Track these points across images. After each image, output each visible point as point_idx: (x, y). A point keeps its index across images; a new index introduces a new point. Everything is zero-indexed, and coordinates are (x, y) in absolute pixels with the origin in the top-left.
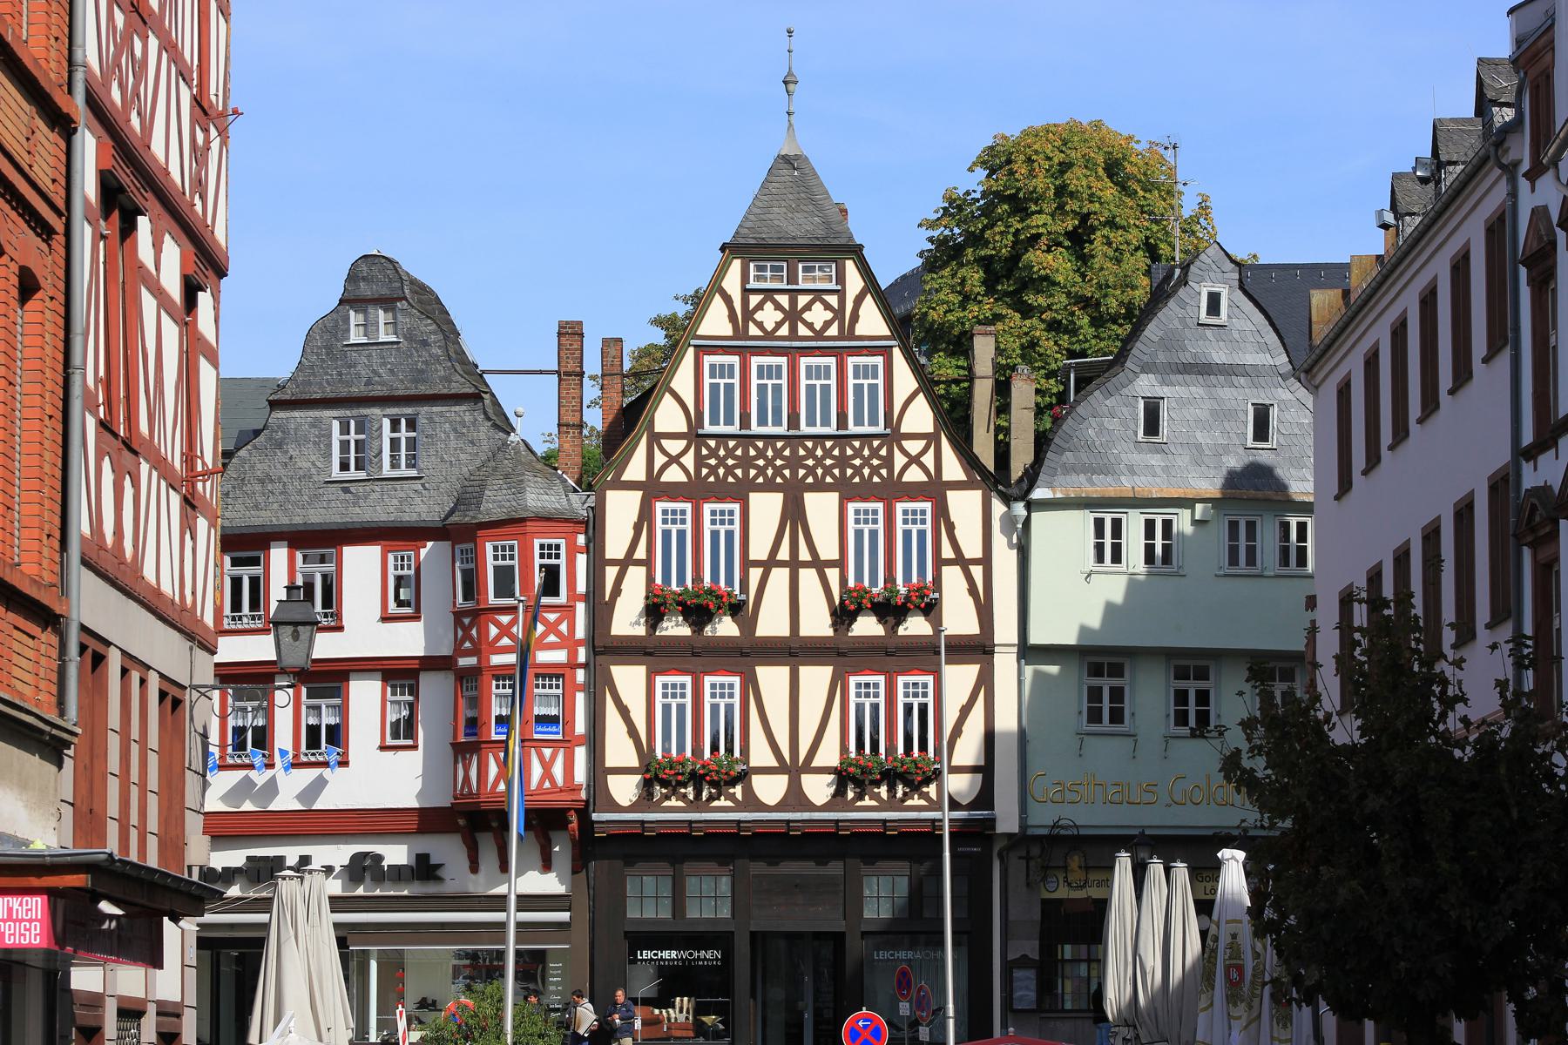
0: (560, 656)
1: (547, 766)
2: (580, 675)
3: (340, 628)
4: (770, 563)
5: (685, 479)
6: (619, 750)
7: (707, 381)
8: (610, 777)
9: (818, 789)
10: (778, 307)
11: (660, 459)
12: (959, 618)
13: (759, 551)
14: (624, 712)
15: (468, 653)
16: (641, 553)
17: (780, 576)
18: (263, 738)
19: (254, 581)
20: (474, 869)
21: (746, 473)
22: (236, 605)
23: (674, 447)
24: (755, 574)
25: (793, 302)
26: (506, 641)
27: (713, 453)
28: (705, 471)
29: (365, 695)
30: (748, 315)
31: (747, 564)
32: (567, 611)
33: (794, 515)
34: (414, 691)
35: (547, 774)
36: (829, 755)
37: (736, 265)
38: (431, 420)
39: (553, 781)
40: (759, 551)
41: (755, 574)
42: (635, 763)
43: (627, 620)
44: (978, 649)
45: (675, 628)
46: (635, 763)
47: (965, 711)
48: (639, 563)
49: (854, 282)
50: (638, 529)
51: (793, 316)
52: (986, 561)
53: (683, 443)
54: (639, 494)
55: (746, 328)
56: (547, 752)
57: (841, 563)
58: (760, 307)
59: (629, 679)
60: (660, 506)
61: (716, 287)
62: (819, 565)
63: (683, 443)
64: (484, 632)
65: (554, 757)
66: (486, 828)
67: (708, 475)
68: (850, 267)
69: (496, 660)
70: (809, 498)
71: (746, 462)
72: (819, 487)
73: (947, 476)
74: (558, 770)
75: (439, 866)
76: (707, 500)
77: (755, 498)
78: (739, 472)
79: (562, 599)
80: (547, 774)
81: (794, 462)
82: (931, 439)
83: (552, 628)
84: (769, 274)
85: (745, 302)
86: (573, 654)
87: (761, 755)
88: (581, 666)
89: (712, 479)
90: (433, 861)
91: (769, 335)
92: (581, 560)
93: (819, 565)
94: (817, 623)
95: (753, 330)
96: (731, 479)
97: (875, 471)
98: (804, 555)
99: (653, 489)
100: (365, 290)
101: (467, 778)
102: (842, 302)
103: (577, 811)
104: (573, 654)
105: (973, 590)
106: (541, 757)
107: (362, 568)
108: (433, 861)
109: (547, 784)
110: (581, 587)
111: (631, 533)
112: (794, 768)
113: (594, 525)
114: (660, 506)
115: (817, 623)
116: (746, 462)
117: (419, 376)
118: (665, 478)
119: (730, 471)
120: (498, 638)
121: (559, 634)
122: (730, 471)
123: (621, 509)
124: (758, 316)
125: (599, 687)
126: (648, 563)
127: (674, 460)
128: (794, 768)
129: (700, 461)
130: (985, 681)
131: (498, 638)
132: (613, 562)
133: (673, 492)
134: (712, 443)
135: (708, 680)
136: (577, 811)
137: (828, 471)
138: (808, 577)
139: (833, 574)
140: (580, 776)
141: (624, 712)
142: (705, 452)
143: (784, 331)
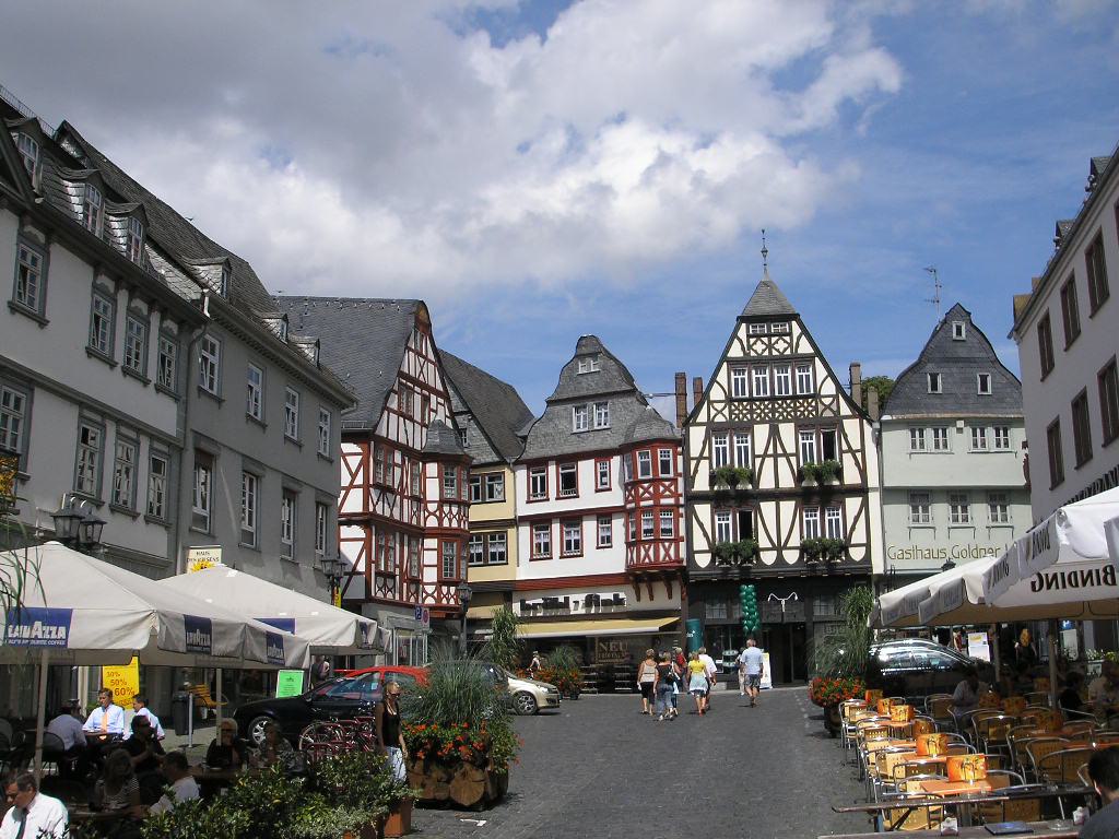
0: (671, 501)
1: (667, 551)
2: (682, 510)
4: (765, 455)
6: (700, 543)
9: (791, 557)
10: (763, 342)
11: (713, 412)
12: (851, 476)
13: (759, 450)
14: (701, 525)
15: (630, 502)
16: (706, 454)
17: (769, 462)
19: (543, 479)
20: (639, 600)
22: (535, 490)
23: (719, 406)
24: (758, 461)
25: (770, 341)
26: (647, 495)
29: (590, 527)
30: (750, 347)
31: (754, 456)
32: (674, 481)
33: (774, 434)
34: (610, 522)
35: (667, 554)
36: (795, 541)
39: (670, 558)
40: (759, 450)
41: (758, 461)
43: (702, 484)
44: (861, 491)
47: (856, 519)
48: (705, 458)
49: (796, 330)
50: (704, 443)
51: (770, 346)
52: (863, 450)
56: (667, 544)
57: (797, 455)
58: (755, 343)
62: (786, 455)
64: (637, 492)
65: (670, 547)
66: (642, 581)
68: (794, 323)
69: (643, 504)
70: (782, 427)
72: (785, 420)
73: (842, 413)
74: (672, 552)
79: (671, 475)
80: (667, 554)
81: (773, 411)
82: (835, 397)
85: (748, 342)
86: (677, 500)
87: (763, 542)
88: (682, 506)
92: (680, 458)
93: (786, 455)
94: (787, 482)
95: (753, 354)
97: (810, 412)
98: (780, 451)
100: (584, 350)
102: (792, 339)
104: (677, 500)
105: (857, 463)
106: (664, 547)
107: (586, 470)
110: (680, 470)
112: (779, 548)
113: (684, 442)
115: (787, 482)
116: (751, 411)
117: (607, 385)
118: (716, 420)
119: (745, 416)
120: (643, 494)
121: (670, 491)
122: (745, 416)
123: (697, 435)
125: (691, 514)
126: (710, 458)
127: (720, 412)
128: (779, 548)
129: (731, 412)
130: (865, 505)
131: (643, 494)
132: (693, 459)
137: (789, 413)
138: (782, 461)
139: (793, 459)
140: (683, 554)
141: (701, 525)
143: (766, 353)
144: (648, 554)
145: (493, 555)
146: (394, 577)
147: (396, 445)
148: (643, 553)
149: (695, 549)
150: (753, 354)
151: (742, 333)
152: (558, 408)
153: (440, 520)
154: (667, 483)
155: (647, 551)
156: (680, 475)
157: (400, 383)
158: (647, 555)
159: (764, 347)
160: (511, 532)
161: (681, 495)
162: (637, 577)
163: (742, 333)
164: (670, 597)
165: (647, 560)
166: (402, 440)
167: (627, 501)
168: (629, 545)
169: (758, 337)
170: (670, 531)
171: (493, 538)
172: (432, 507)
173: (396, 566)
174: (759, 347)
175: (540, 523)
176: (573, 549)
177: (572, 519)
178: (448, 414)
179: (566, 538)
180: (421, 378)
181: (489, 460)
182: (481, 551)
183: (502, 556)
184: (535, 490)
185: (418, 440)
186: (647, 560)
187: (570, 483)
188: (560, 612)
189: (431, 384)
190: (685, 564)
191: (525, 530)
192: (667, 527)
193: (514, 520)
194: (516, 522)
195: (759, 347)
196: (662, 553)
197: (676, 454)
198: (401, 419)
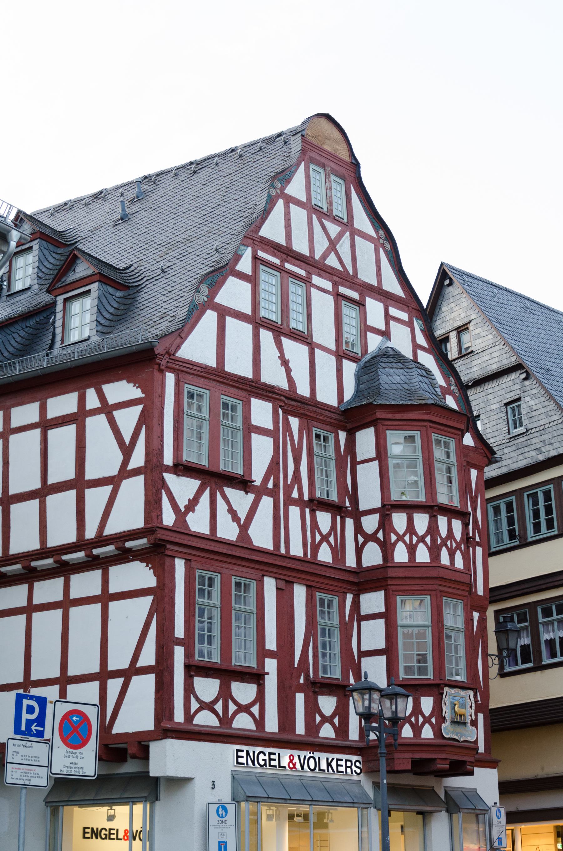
146: (256, 677)
147: (255, 388)
153: (387, 549)
157: (255, 258)
166: (273, 375)
172: (370, 523)
173: (263, 653)
178: (421, 340)
180: (332, 261)
185: (332, 385)
189: (367, 275)
198: (266, 336)
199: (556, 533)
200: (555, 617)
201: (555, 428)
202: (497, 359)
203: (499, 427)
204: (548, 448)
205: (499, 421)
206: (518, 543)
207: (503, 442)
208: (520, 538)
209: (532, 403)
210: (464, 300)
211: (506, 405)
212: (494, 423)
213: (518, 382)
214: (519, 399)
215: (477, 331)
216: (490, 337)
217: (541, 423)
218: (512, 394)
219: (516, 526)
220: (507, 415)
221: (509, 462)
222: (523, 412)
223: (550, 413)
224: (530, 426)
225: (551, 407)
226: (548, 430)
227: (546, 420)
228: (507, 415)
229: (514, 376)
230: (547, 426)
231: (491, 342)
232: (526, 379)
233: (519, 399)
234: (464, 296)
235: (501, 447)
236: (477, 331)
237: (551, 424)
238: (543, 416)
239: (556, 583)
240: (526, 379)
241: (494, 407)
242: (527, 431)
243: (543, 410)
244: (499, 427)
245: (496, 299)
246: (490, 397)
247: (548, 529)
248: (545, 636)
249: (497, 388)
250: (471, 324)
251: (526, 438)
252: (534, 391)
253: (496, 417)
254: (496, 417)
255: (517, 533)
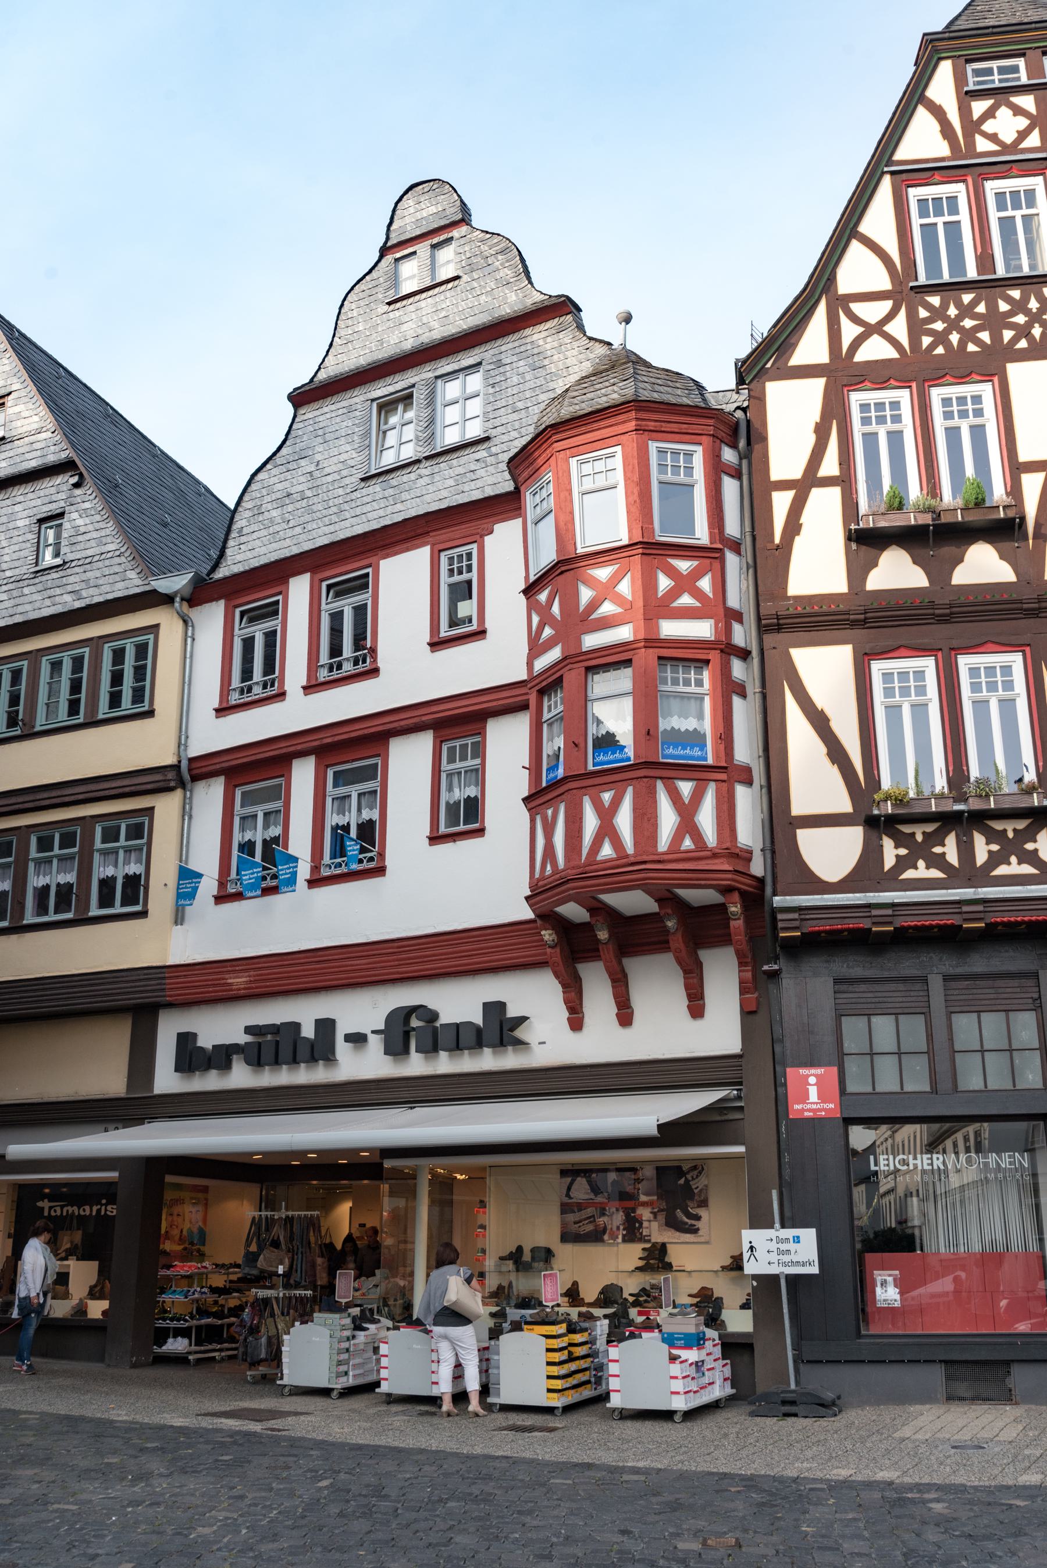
0: (702, 629)
1: (687, 812)
3: (374, 672)
5: (892, 354)
6: (814, 783)
7: (916, 222)
8: (800, 833)
10: (1018, 111)
11: (849, 331)
14: (820, 722)
16: (830, 466)
18: (273, 851)
19: (270, 637)
20: (576, 1023)
21: (996, 337)
22: (247, 673)
23: (872, 312)
27: (938, 314)
28: (926, 341)
29: (410, 761)
30: (972, 127)
34: (479, 750)
35: (687, 824)
37: (945, 70)
38: (499, 364)
42: (844, 805)
45: (896, 572)
46: (844, 805)
48: (828, 482)
50: (821, 432)
53: (887, 305)
54: (818, 384)
55: (971, 144)
56: (685, 788)
58: (990, 114)
59: (824, 668)
60: (856, 398)
61: (915, 95)
63: (887, 305)
65: (697, 797)
67: (932, 346)
69: (591, 641)
71: (994, 321)
74: (706, 819)
75: (523, 1019)
76: (938, 380)
77: (1015, 371)
78: (985, 336)
80: (687, 824)
83: (685, 583)
84: (996, 77)
85: (964, 111)
88: (744, 654)
89: (940, 350)
90: (512, 1012)
91: (1006, 148)
95: (983, 145)
96: (971, 348)
99: (842, 375)
101: (549, 848)
103: (743, 894)
106: (675, 797)
108: (512, 1012)
109: (688, 843)
111: (812, 439)
114: (856, 398)
116: (994, 321)
118: (861, 356)
121: (698, 594)
124: (988, 127)
125: (776, 681)
126: (845, 481)
127: (877, 329)
129: (916, 328)
132: (784, 485)
133: (878, 375)
134: (935, 300)
135: (965, 662)
136: (743, 894)
140: (748, 831)
141: (820, 722)
142: (923, 313)
144: (613, 825)
145: (107, 884)
148: (591, 822)
149: (799, 807)
150: (983, 145)
151: (942, 87)
152: (327, 413)
154: (684, 566)
155: (606, 816)
156: (736, 546)
158: (607, 830)
159: (1023, 123)
160: (166, 808)
161: (738, 616)
162: (582, 930)
163: (942, 87)
164: (697, 1009)
165: (607, 851)
167: (536, 648)
168: (537, 800)
169: (1001, 94)
170: (696, 738)
171: (110, 835)
174: (1006, 125)
175: (252, 770)
176: (356, 853)
177: (353, 749)
179: (332, 819)
181: (119, 590)
182: (69, 877)
183: (135, 888)
184: (247, 673)
186: (607, 851)
187: (349, 652)
188: (303, 1076)
190: (757, 868)
191: (210, 797)
192: (688, 724)
193: (176, 767)
194: (184, 775)
195: (1006, 125)
196: (668, 819)
197: (716, 470)
199: (81, 721)
200: (56, 851)
201: (107, 562)
202: (39, 453)
203: (23, 554)
204: (91, 591)
205: (24, 545)
206: (19, 732)
207: (25, 577)
208: (24, 724)
209: (80, 522)
210: (7, 362)
211: (41, 521)
212: (17, 548)
213: (65, 489)
214: (61, 515)
215: (17, 409)
216: (36, 418)
217: (89, 552)
218: (53, 506)
219: (21, 708)
220: (39, 538)
221: (28, 607)
222: (65, 535)
223: (104, 540)
224: (70, 557)
225: (108, 532)
226: (95, 565)
227: (97, 550)
228: (39, 538)
229: (59, 480)
230: (96, 558)
231: (35, 426)
232: (77, 485)
233: (61, 515)
234: (8, 356)
235: (21, 584)
236: (17, 409)
237: (103, 556)
238: (93, 543)
239: (67, 799)
240: (77, 485)
241: (20, 523)
242: (65, 563)
243: (95, 535)
244: (23, 554)
245: (60, 381)
246: (17, 508)
247: (70, 714)
248: (36, 881)
249: (31, 496)
250: (10, 397)
251: (61, 573)
252: (87, 505)
253: (21, 539)
254: (21, 539)
255: (20, 717)
